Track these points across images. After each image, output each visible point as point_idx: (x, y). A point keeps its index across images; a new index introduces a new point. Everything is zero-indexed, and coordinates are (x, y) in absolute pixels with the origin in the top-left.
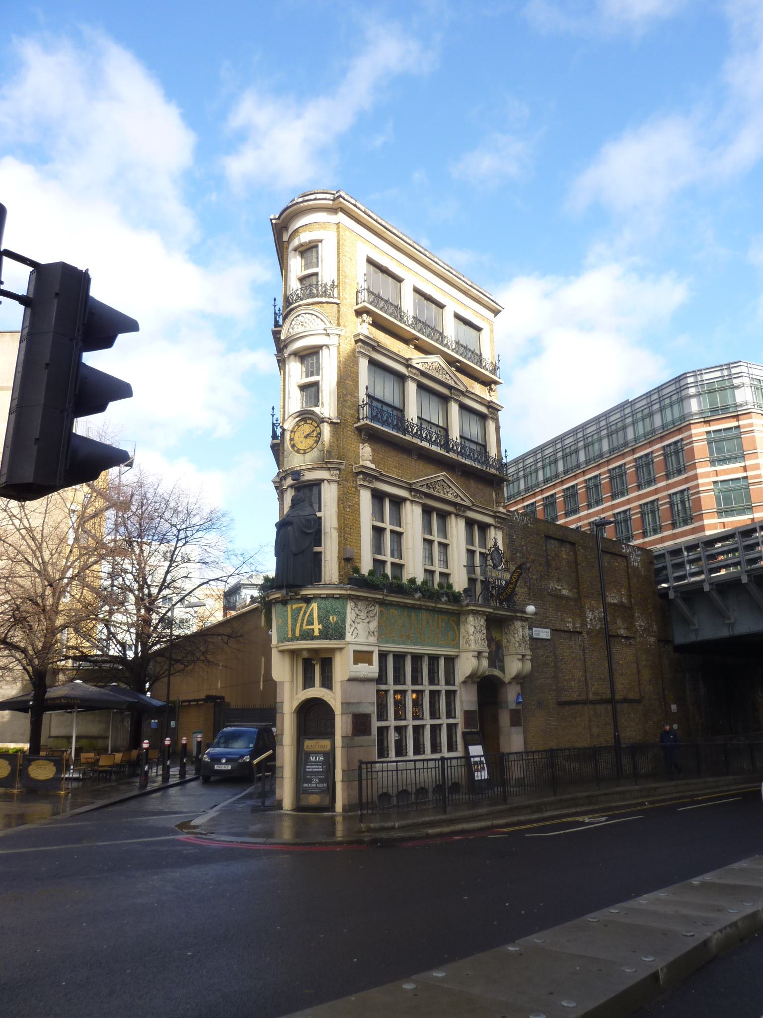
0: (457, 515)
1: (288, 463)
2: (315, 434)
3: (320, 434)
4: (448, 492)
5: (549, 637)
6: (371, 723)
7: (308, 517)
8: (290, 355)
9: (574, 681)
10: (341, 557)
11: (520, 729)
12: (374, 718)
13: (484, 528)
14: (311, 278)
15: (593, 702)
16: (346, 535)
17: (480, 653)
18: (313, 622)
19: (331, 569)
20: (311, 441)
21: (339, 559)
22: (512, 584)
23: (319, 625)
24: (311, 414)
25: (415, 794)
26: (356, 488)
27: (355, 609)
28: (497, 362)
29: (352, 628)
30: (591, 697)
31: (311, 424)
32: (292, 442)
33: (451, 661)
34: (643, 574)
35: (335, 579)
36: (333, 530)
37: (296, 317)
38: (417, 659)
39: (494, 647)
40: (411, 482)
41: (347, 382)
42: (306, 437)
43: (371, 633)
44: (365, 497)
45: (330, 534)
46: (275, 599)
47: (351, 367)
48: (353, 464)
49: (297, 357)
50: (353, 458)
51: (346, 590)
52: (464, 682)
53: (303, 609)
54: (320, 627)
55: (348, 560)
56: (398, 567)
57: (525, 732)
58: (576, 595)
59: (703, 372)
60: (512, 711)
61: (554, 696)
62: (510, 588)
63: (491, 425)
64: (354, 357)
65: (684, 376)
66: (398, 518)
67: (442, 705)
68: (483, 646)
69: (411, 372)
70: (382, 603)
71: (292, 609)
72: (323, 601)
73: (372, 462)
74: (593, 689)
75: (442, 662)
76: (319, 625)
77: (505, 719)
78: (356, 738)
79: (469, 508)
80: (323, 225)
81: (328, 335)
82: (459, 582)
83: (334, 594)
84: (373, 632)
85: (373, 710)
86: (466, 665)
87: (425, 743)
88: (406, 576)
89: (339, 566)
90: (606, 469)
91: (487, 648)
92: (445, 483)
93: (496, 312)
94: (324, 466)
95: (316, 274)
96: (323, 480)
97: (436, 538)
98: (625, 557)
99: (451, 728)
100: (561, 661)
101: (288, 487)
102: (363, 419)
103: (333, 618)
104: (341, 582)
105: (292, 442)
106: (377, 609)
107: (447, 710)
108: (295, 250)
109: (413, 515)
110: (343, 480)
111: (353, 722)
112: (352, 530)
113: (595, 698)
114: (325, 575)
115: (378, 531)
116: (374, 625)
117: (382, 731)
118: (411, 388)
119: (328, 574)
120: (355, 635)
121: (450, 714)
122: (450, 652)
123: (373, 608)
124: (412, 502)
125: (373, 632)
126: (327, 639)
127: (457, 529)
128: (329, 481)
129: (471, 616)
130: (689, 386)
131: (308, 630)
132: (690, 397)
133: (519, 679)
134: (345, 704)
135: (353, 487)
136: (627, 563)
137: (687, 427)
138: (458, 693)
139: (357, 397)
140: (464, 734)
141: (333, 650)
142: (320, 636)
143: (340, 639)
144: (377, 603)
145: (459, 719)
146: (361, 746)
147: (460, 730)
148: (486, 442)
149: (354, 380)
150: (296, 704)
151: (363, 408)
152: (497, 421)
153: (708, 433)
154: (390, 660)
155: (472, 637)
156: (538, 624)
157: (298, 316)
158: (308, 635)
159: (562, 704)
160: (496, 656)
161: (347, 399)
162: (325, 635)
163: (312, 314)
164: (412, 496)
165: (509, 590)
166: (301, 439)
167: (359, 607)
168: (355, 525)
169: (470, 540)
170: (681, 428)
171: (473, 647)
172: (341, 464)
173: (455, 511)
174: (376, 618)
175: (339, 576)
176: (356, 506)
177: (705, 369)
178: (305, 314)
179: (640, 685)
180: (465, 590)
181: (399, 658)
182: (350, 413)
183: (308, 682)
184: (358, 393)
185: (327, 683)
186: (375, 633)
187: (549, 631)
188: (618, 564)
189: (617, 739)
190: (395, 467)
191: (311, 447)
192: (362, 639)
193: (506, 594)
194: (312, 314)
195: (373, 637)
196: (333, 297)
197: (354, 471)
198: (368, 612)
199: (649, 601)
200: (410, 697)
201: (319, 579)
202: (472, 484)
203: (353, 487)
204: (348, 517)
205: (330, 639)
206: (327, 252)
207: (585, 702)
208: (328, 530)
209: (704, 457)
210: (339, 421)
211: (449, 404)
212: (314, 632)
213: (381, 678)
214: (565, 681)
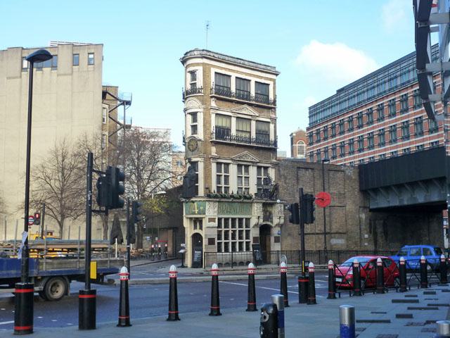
11: (279, 244)
12: (216, 239)
13: (266, 168)
15: (317, 234)
19: (201, 192)
30: (317, 231)
33: (248, 220)
35: (203, 195)
38: (233, 220)
39: (268, 214)
44: (214, 166)
55: (207, 188)
56: (227, 189)
57: (281, 245)
63: (272, 126)
68: (261, 215)
70: (219, 202)
75: (244, 220)
77: (272, 239)
80: (198, 64)
82: (253, 190)
86: (253, 221)
88: (230, 192)
90: (398, 95)
93: (277, 75)
97: (243, 175)
98: (343, 171)
99: (248, 243)
106: (217, 203)
109: (233, 169)
113: (319, 232)
115: (219, 177)
116: (216, 209)
117: (219, 244)
118: (234, 120)
122: (248, 217)
127: (253, 171)
133: (281, 226)
140: (253, 245)
145: (251, 240)
147: (251, 243)
150: (191, 234)
154: (223, 220)
158: (194, 213)
160: (268, 216)
162: (199, 213)
169: (259, 173)
180: (255, 194)
181: (227, 220)
183: (195, 228)
185: (201, 228)
188: (340, 175)
189: (325, 248)
192: (212, 214)
200: (230, 233)
201: (197, 194)
202: (261, 152)
206: (200, 75)
207: (313, 234)
213: (219, 226)
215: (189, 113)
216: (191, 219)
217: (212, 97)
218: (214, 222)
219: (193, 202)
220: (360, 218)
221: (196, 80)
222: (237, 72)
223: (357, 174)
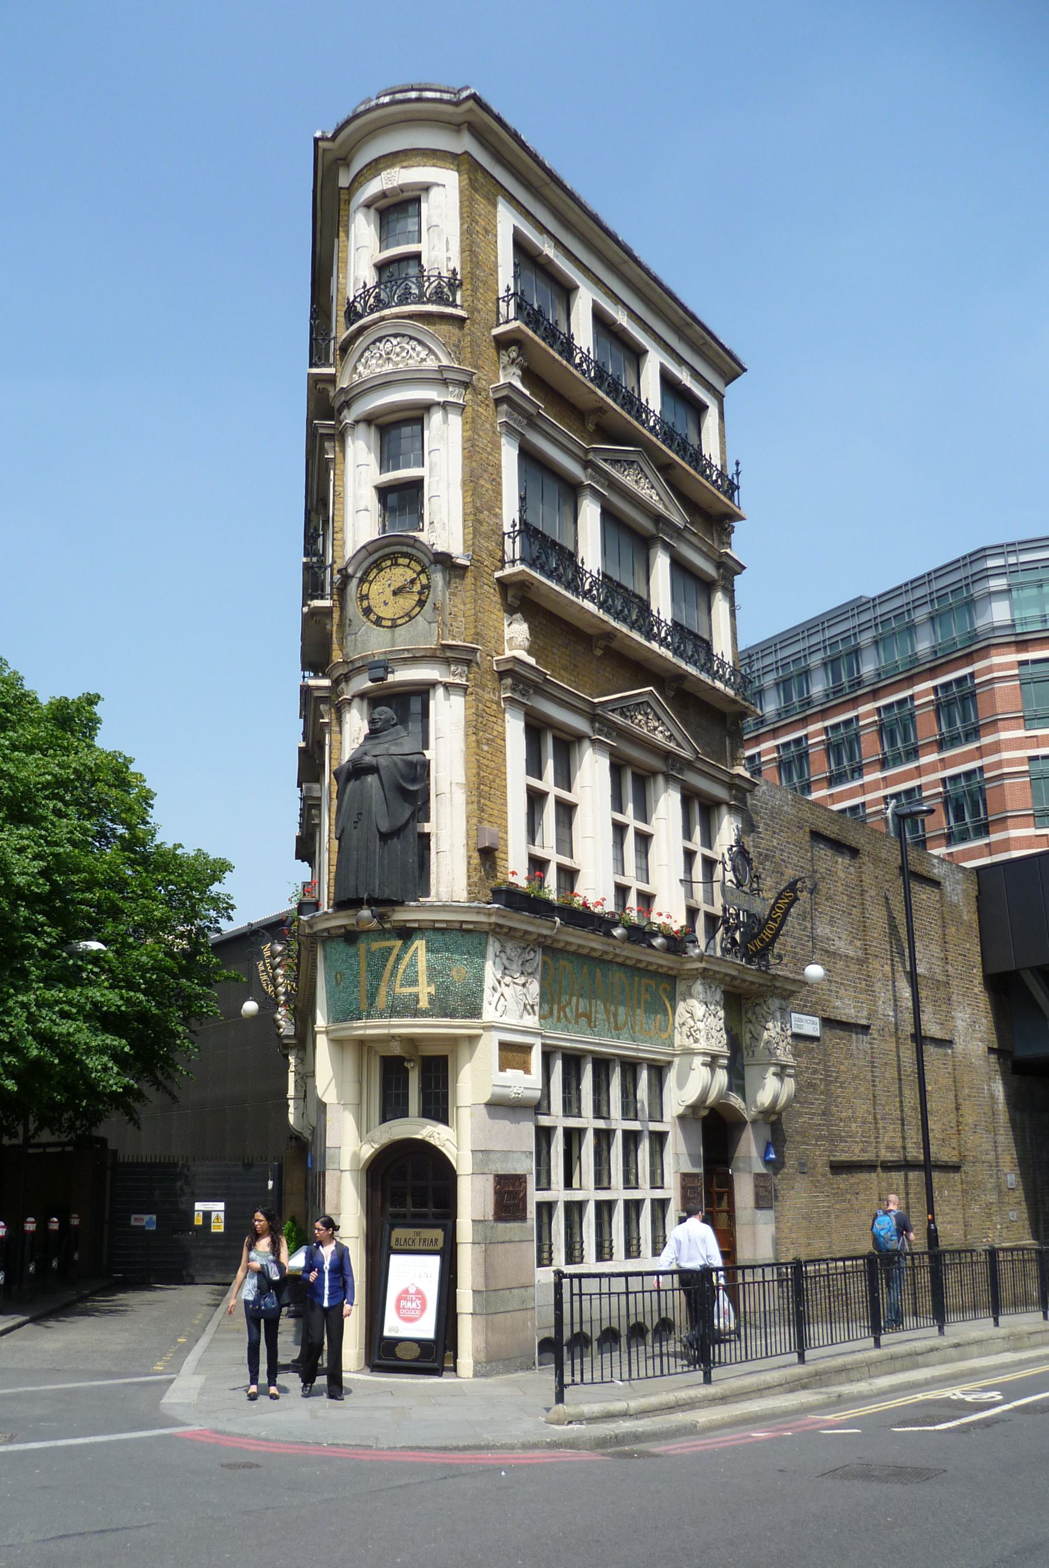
0: (668, 778)
1: (356, 644)
2: (417, 587)
3: (426, 587)
4: (655, 728)
5: (817, 1034)
6: (525, 1194)
7: (409, 757)
8: (357, 422)
9: (855, 1122)
10: (472, 846)
14: (404, 264)
16: (482, 801)
17: (714, 1057)
18: (417, 981)
20: (408, 602)
21: (468, 851)
22: (774, 920)
23: (429, 985)
24: (408, 545)
25: (598, 1340)
26: (498, 704)
27: (502, 955)
28: (735, 476)
29: (497, 995)
30: (886, 1155)
31: (408, 566)
32: (365, 603)
34: (965, 918)
36: (454, 787)
37: (374, 343)
38: (602, 1065)
40: (596, 700)
41: (482, 482)
42: (395, 593)
43: (528, 1007)
46: (327, 930)
47: (489, 454)
48: (494, 654)
49: (373, 429)
50: (493, 642)
51: (490, 915)
52: (681, 1118)
53: (395, 952)
54: (432, 989)
58: (860, 953)
59: (1018, 547)
60: (758, 1176)
61: (825, 1150)
62: (771, 929)
63: (720, 604)
64: (494, 432)
65: (982, 554)
66: (565, 774)
67: (644, 1161)
69: (592, 478)
71: (368, 951)
72: (439, 936)
73: (530, 652)
74: (886, 1139)
76: (429, 985)
78: (501, 1226)
79: (688, 765)
81: (445, 382)
83: (462, 922)
84: (532, 1006)
85: (527, 1166)
87: (614, 1237)
89: (469, 863)
90: (819, 725)
91: (725, 1049)
92: (652, 709)
94: (438, 653)
95: (417, 257)
96: (433, 684)
98: (936, 884)
100: (836, 1082)
101: (354, 697)
102: (513, 562)
104: (472, 896)
105: (365, 603)
107: (651, 1170)
108: (368, 206)
110: (476, 686)
111: (496, 1192)
112: (492, 791)
114: (438, 882)
115: (535, 799)
119: (445, 879)
120: (500, 1008)
121: (657, 1183)
123: (532, 954)
124: (594, 742)
125: (532, 1006)
126: (445, 1016)
128: (447, 686)
129: (699, 982)
130: (990, 573)
132: (991, 595)
134: (482, 1155)
135: (492, 701)
136: (941, 898)
137: (982, 653)
138: (670, 1138)
139: (498, 516)
141: (455, 1040)
142: (431, 1010)
143: (472, 1018)
144: (540, 945)
146: (510, 1242)
148: (711, 635)
149: (494, 480)
150: (367, 1151)
151: (514, 538)
152: (730, 594)
153: (1022, 663)
155: (701, 1025)
156: (798, 1005)
159: (838, 1168)
161: (481, 517)
162: (442, 1007)
163: (411, 338)
164: (594, 731)
165: (768, 933)
166: (383, 598)
167: (508, 951)
168: (498, 781)
170: (971, 653)
171: (702, 1045)
172: (475, 650)
173: (665, 769)
174: (538, 977)
175: (469, 885)
176: (499, 742)
177: (1020, 543)
178: (395, 336)
179: (959, 1132)
181: (573, 1061)
182: (487, 548)
184: (501, 509)
186: (536, 1008)
187: (817, 1020)
190: (565, 669)
191: (407, 614)
192: (511, 1020)
193: (762, 940)
194: (411, 338)
195: (532, 1016)
196: (456, 306)
197: (495, 668)
198: (522, 964)
199: (975, 971)
203: (492, 701)
204: (486, 762)
205: (452, 1016)
208: (444, 787)
209: (1014, 709)
210: (468, 563)
211: (652, 552)
212: (418, 1003)
214: (841, 1120)
215: (369, 420)
216: (363, 1045)
217: (502, 343)
218: (527, 1071)
219: (406, 933)
220: (992, 1097)
221: (315, 381)
222: (598, 281)
223: (974, 907)
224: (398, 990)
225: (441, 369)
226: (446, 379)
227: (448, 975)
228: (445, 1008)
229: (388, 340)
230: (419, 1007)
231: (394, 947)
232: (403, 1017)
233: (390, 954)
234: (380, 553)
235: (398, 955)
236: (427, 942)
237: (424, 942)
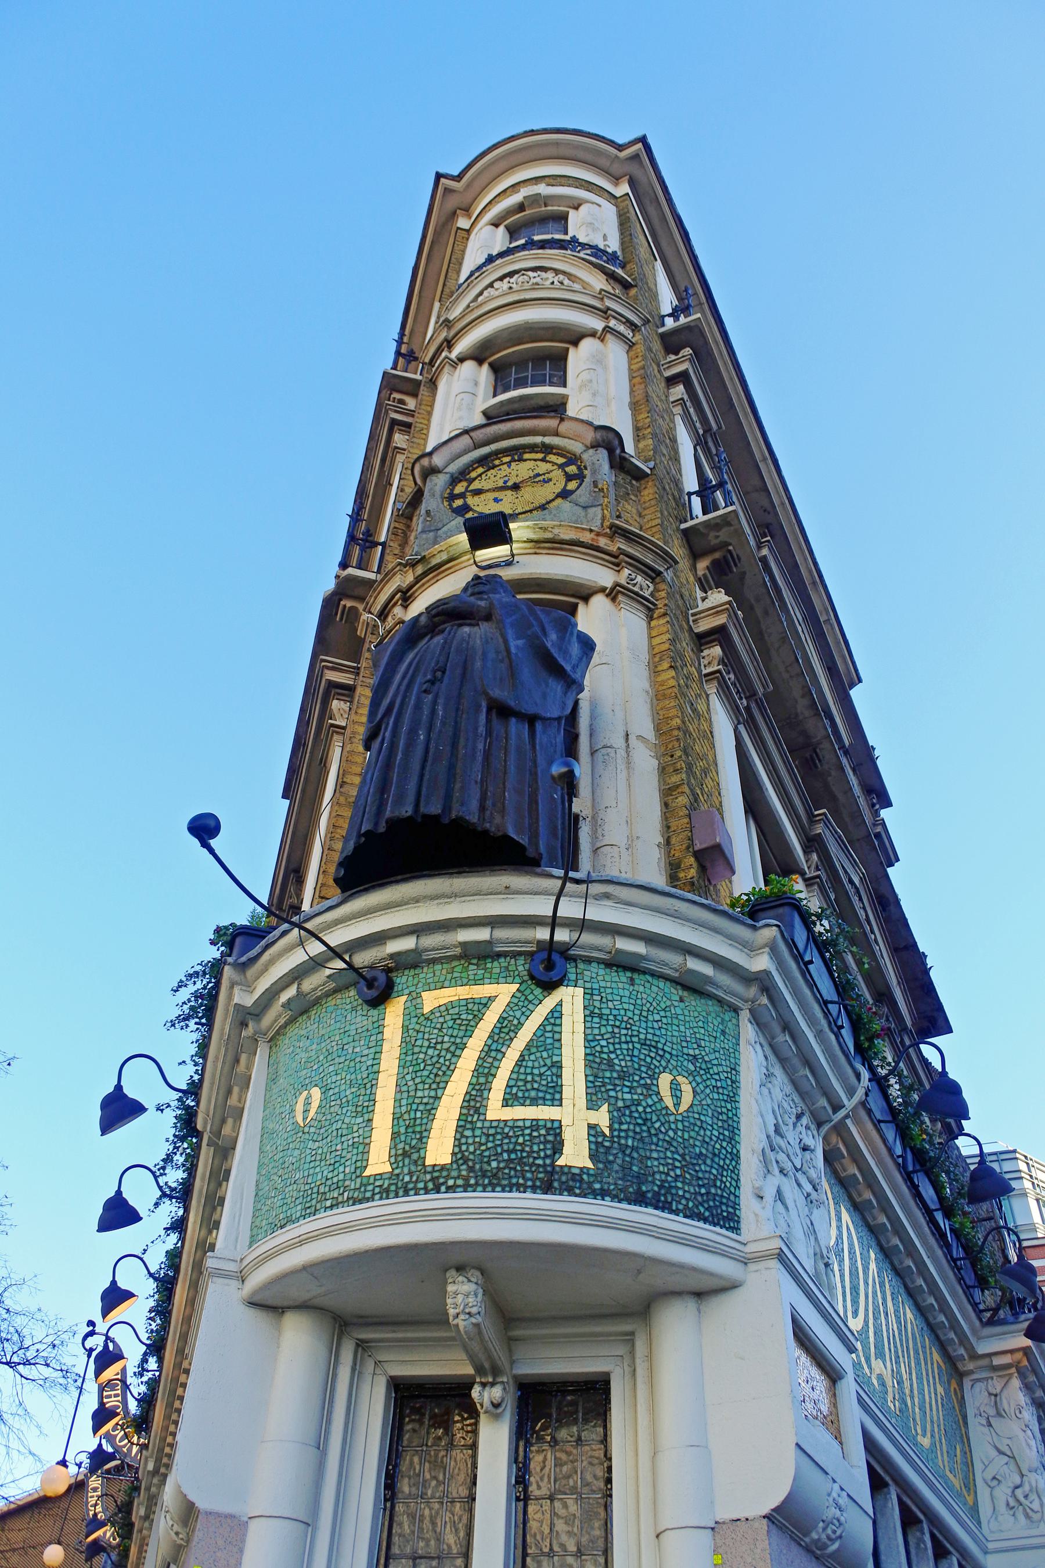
23: (592, 1105)
31: (543, 460)
45: (622, 753)
54: (602, 1118)
71: (413, 1013)
76: (592, 1105)
94: (603, 542)
103: (675, 1088)
126: (640, 1199)
131: (515, 1125)
142: (597, 1176)
157: (511, 274)
194: (557, 271)
212: (558, 1148)
224: (495, 1110)
225: (602, 295)
226: (609, 309)
227: (646, 1086)
228: (641, 1179)
229: (523, 275)
230: (561, 1162)
231: (491, 999)
232: (511, 1187)
233: (478, 1017)
234: (494, 447)
235: (502, 1019)
236: (589, 993)
237: (580, 991)
